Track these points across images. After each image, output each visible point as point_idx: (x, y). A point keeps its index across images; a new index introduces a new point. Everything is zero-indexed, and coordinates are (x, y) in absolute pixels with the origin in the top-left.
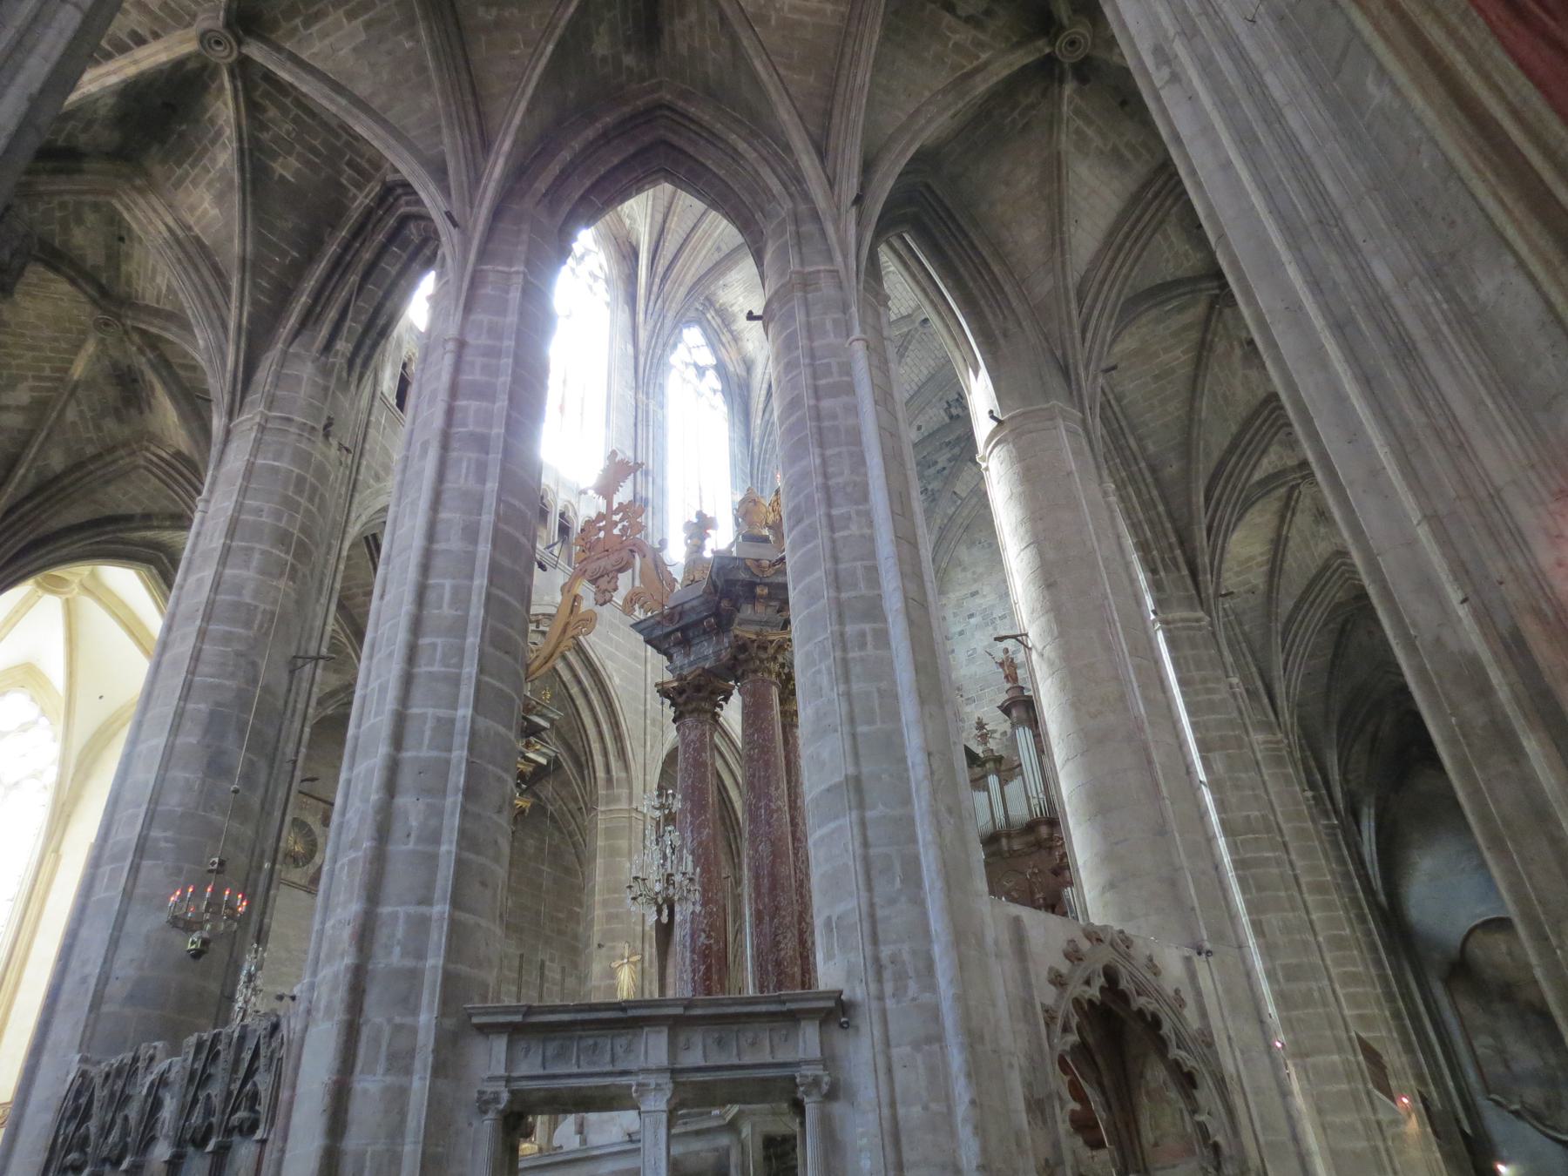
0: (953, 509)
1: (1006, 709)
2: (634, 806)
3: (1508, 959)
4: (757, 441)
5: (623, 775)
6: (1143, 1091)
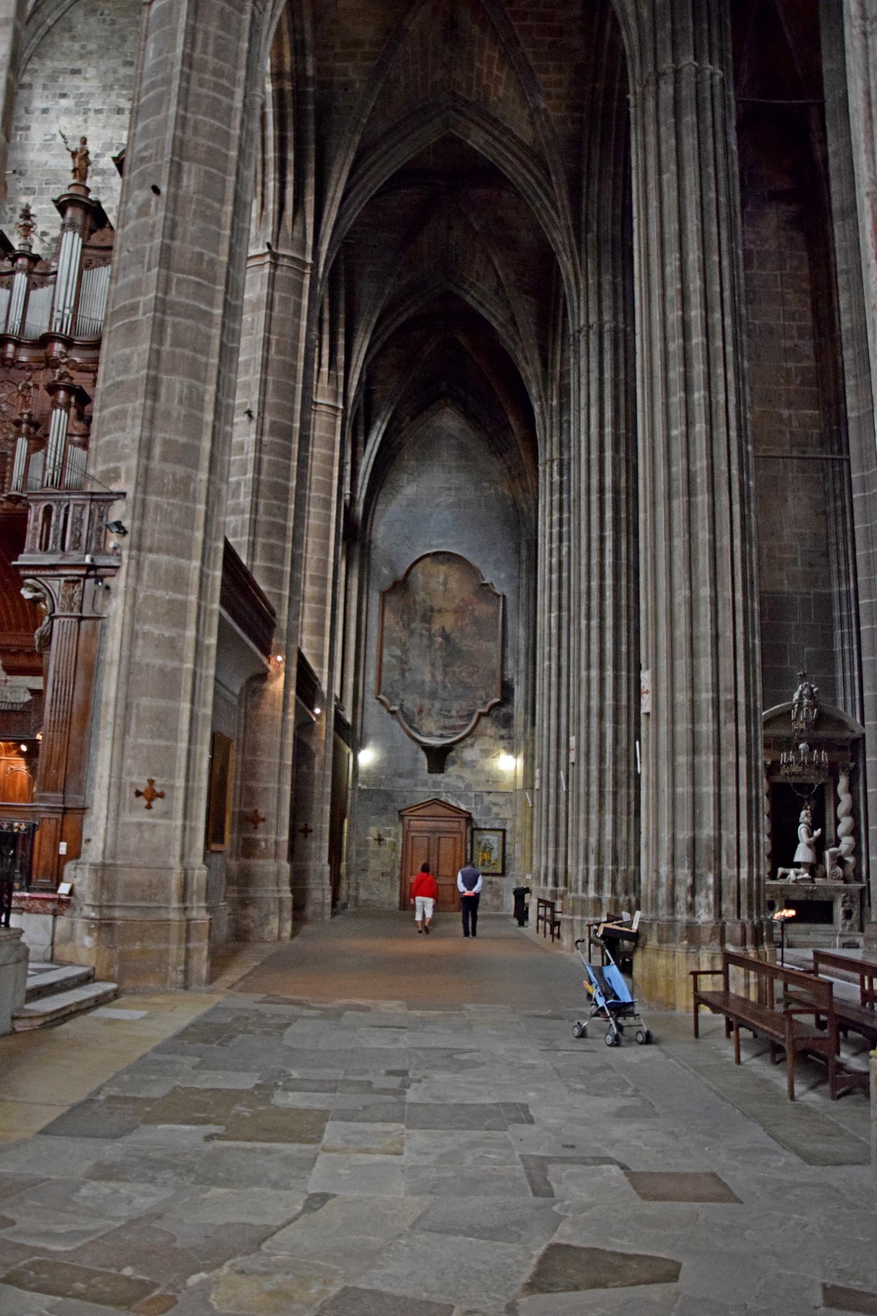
1: (62, 206)
3: (441, 588)
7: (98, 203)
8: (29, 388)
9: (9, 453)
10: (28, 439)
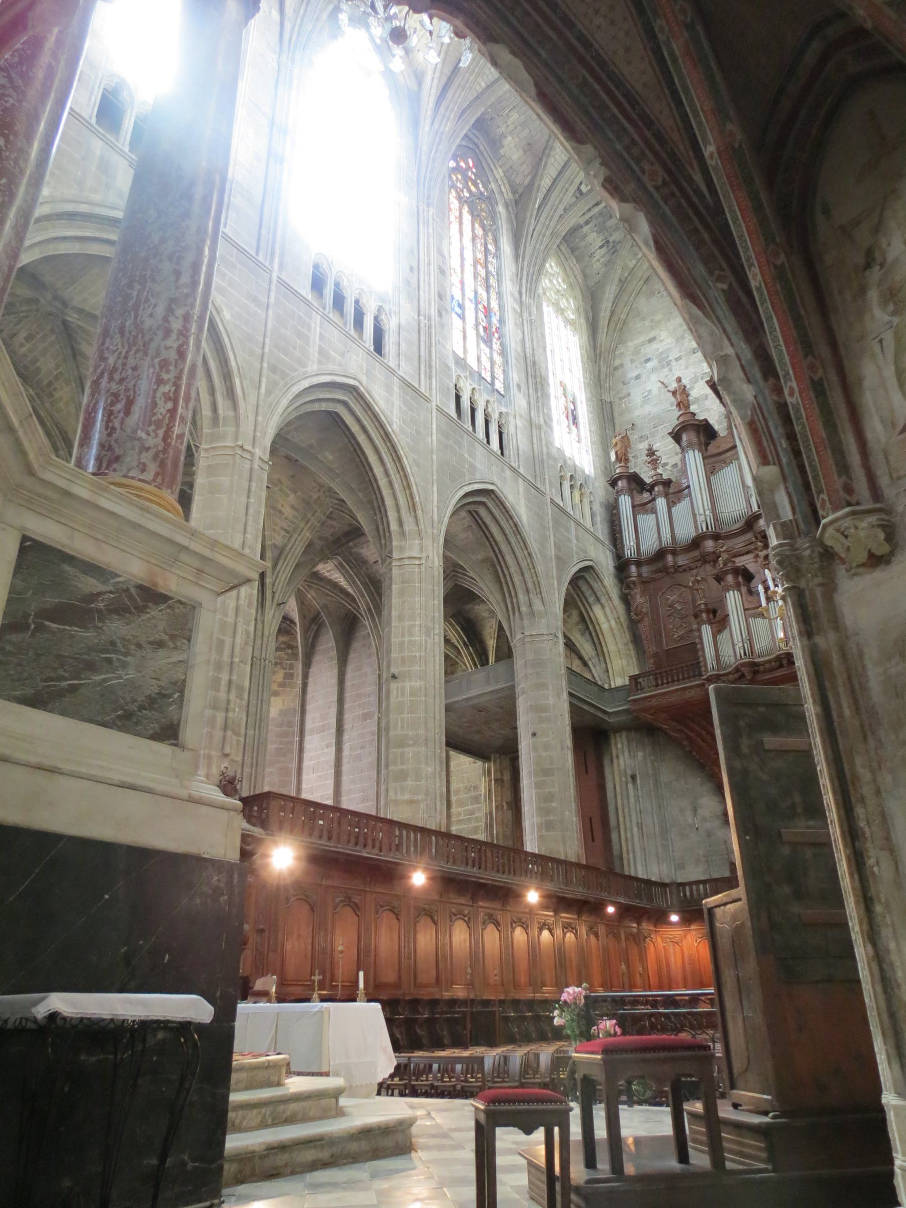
0: (634, 262)
1: (676, 436)
2: (240, 443)
4: (425, 148)
5: (231, 413)
6: (873, 295)
7: (706, 420)
8: (698, 581)
9: (697, 641)
10: (710, 624)
